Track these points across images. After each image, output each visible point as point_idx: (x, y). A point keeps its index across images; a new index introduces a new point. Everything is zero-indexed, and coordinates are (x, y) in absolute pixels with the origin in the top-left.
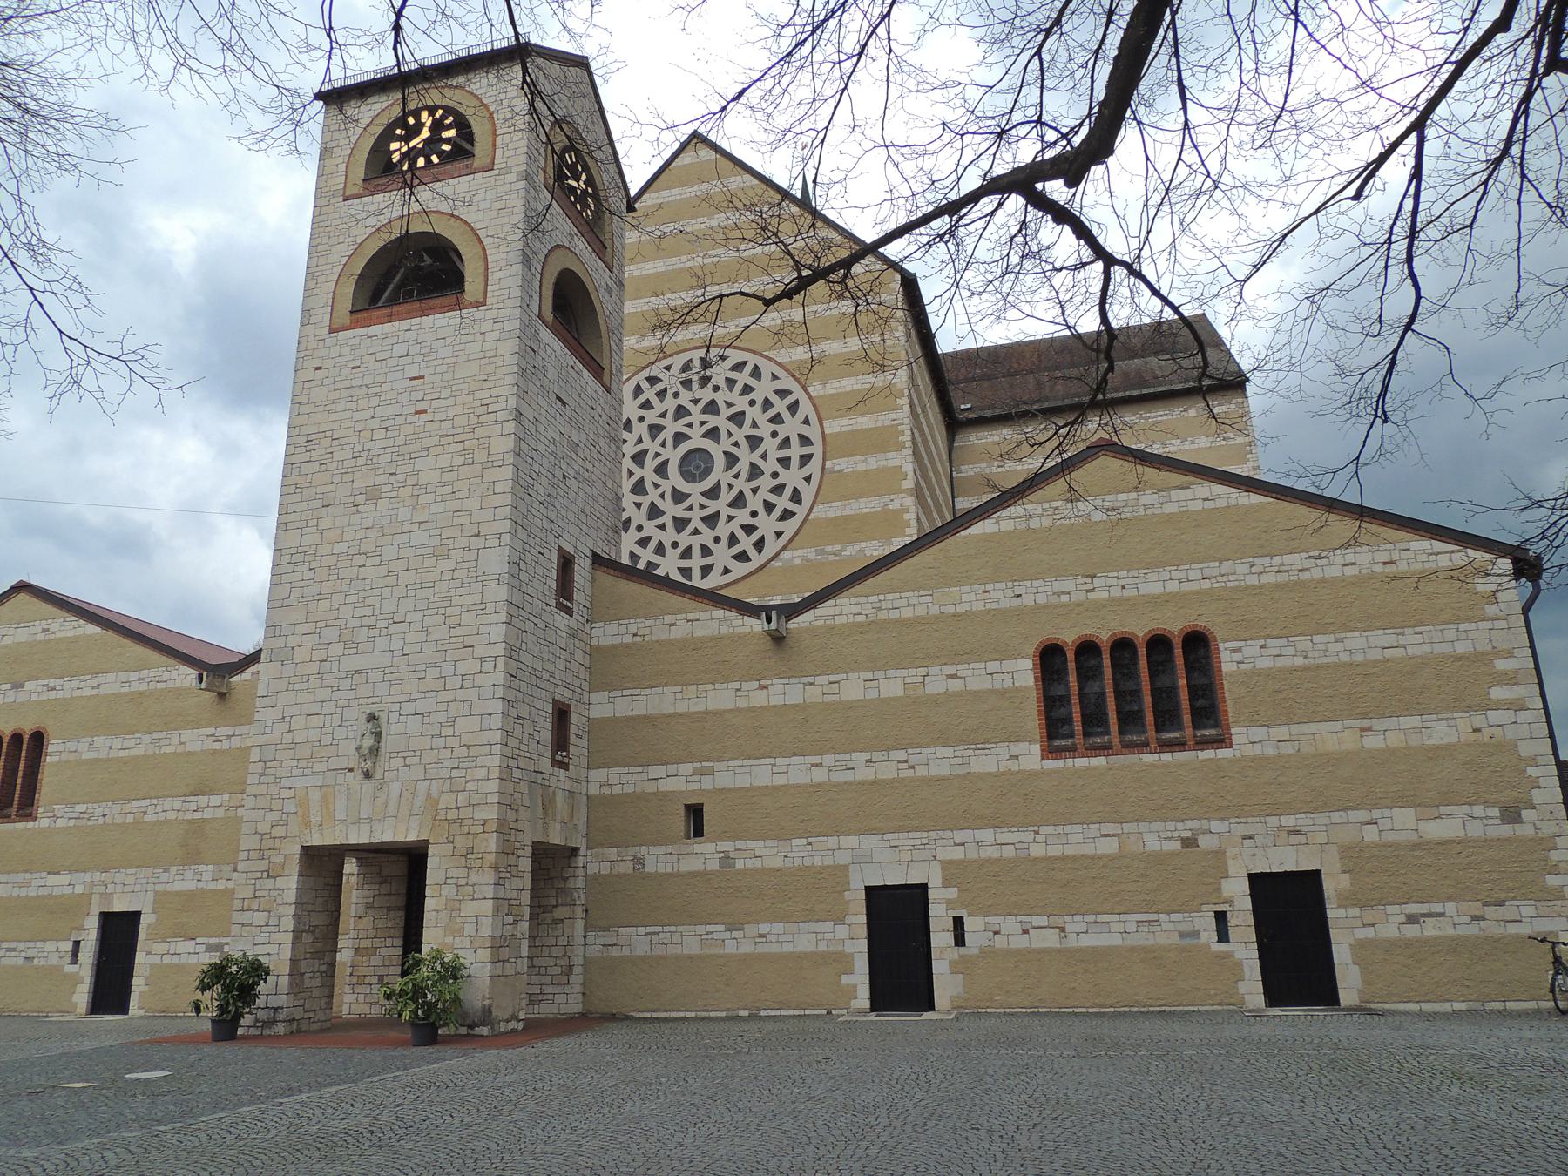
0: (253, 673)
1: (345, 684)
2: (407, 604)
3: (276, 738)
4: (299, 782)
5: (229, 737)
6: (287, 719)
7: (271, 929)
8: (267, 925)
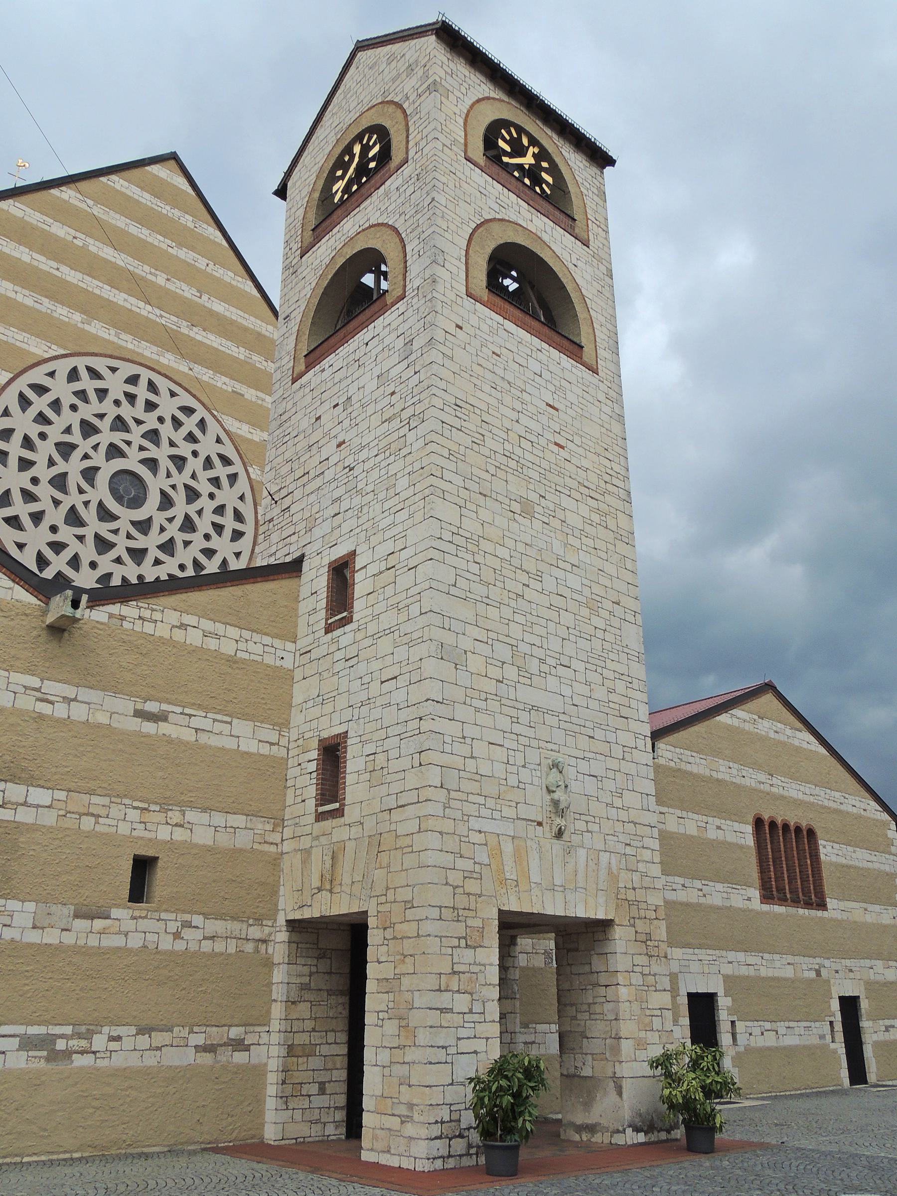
0: (111, 616)
1: (524, 717)
2: (570, 649)
3: (459, 762)
4: (488, 826)
5: (68, 700)
6: (468, 741)
7: (476, 1017)
8: (471, 1012)
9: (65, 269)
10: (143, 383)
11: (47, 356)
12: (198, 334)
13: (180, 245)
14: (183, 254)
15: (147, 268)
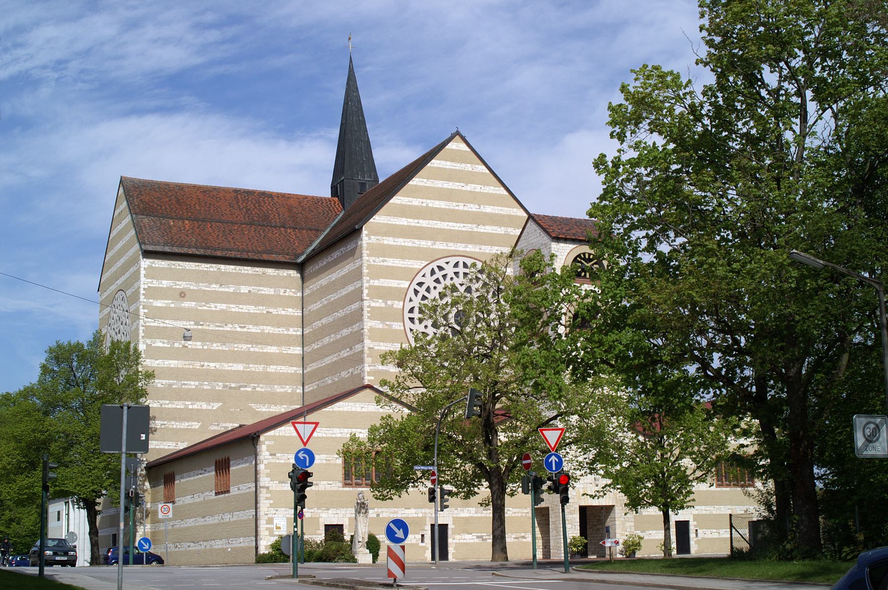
9: (421, 221)
10: (461, 264)
11: (421, 267)
12: (482, 229)
13: (467, 184)
14: (469, 187)
15: (454, 204)
